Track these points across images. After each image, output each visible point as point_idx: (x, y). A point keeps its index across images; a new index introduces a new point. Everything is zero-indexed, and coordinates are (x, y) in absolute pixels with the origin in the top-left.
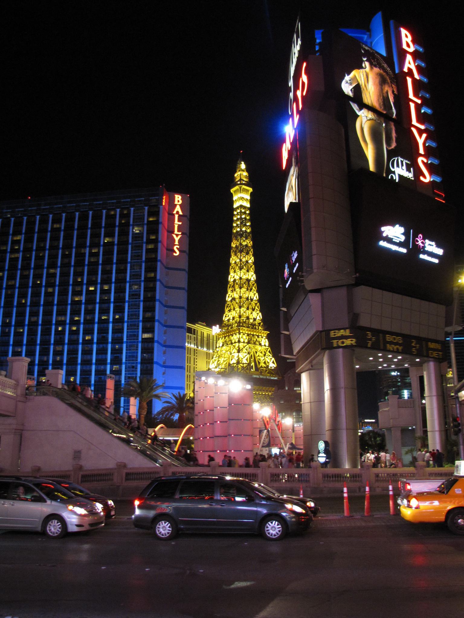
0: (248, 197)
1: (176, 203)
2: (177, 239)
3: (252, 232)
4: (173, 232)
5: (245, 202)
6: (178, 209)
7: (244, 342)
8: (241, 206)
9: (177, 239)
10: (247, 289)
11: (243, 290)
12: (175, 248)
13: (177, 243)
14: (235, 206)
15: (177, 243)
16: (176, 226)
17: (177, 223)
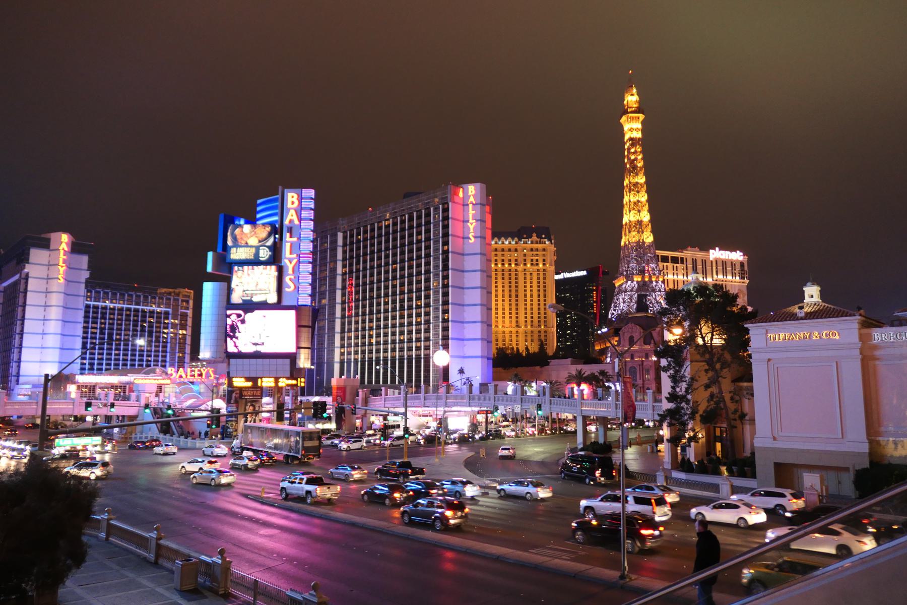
0: (639, 126)
1: (470, 193)
2: (471, 227)
3: (644, 166)
4: (468, 221)
5: (635, 132)
6: (472, 199)
7: (631, 291)
8: (631, 139)
9: (471, 227)
10: (638, 232)
11: (634, 233)
12: (470, 236)
13: (472, 230)
14: (626, 138)
15: (472, 230)
16: (471, 216)
17: (471, 212)
